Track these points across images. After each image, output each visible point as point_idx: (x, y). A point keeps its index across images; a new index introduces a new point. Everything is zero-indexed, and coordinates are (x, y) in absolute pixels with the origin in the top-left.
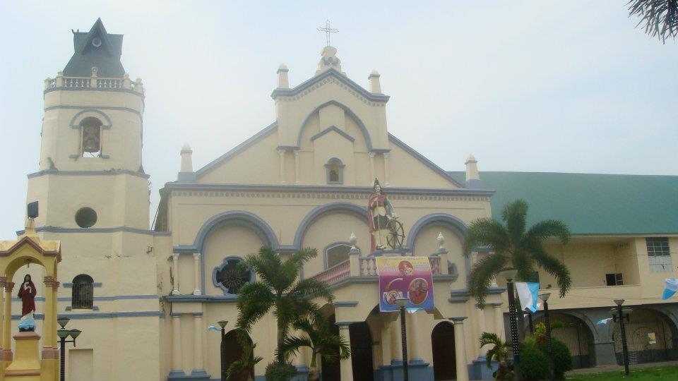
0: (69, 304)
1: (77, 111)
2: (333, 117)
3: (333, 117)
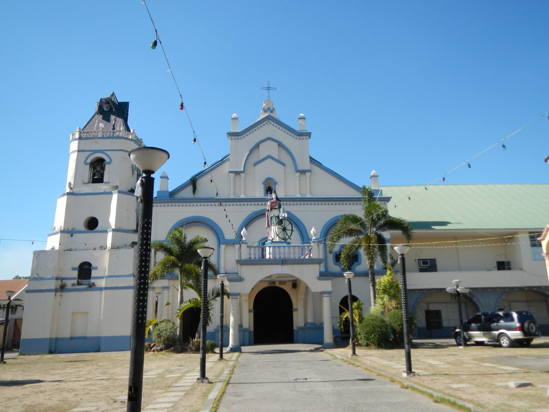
0: (75, 281)
1: (89, 153)
2: (269, 149)
3: (269, 149)
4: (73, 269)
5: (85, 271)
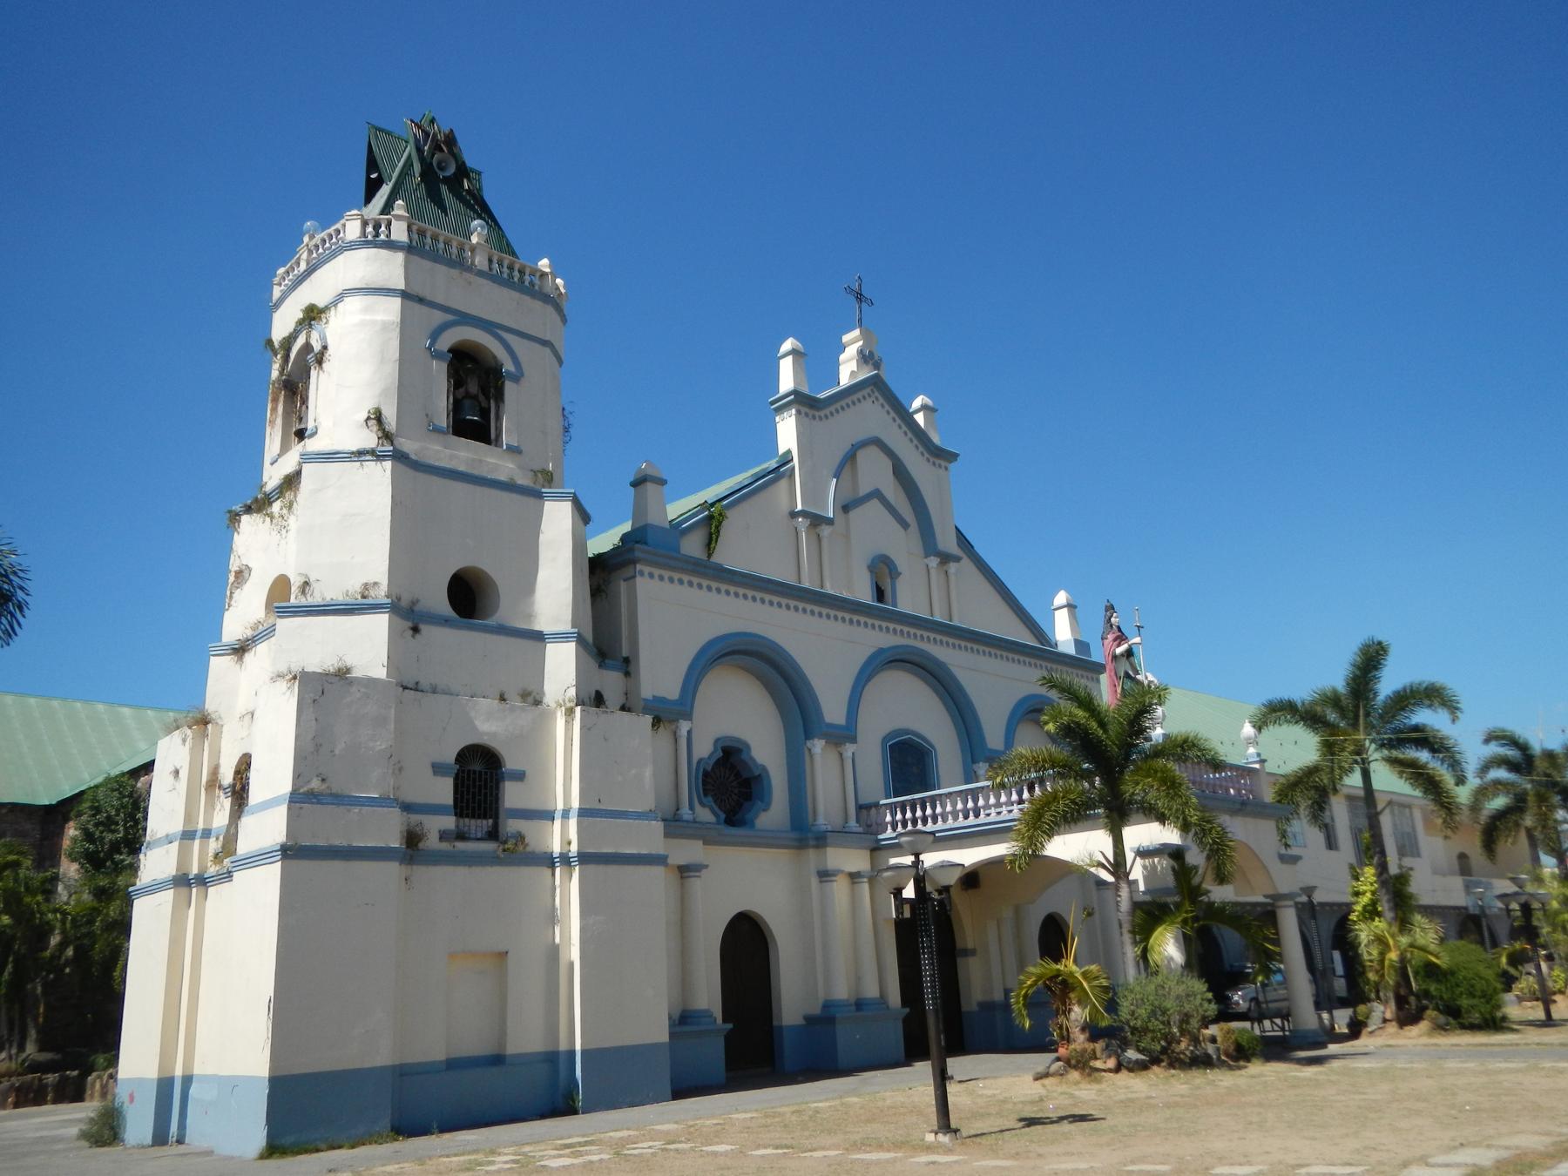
1: (439, 317)
2: (874, 472)
4: (438, 769)
5: (480, 781)
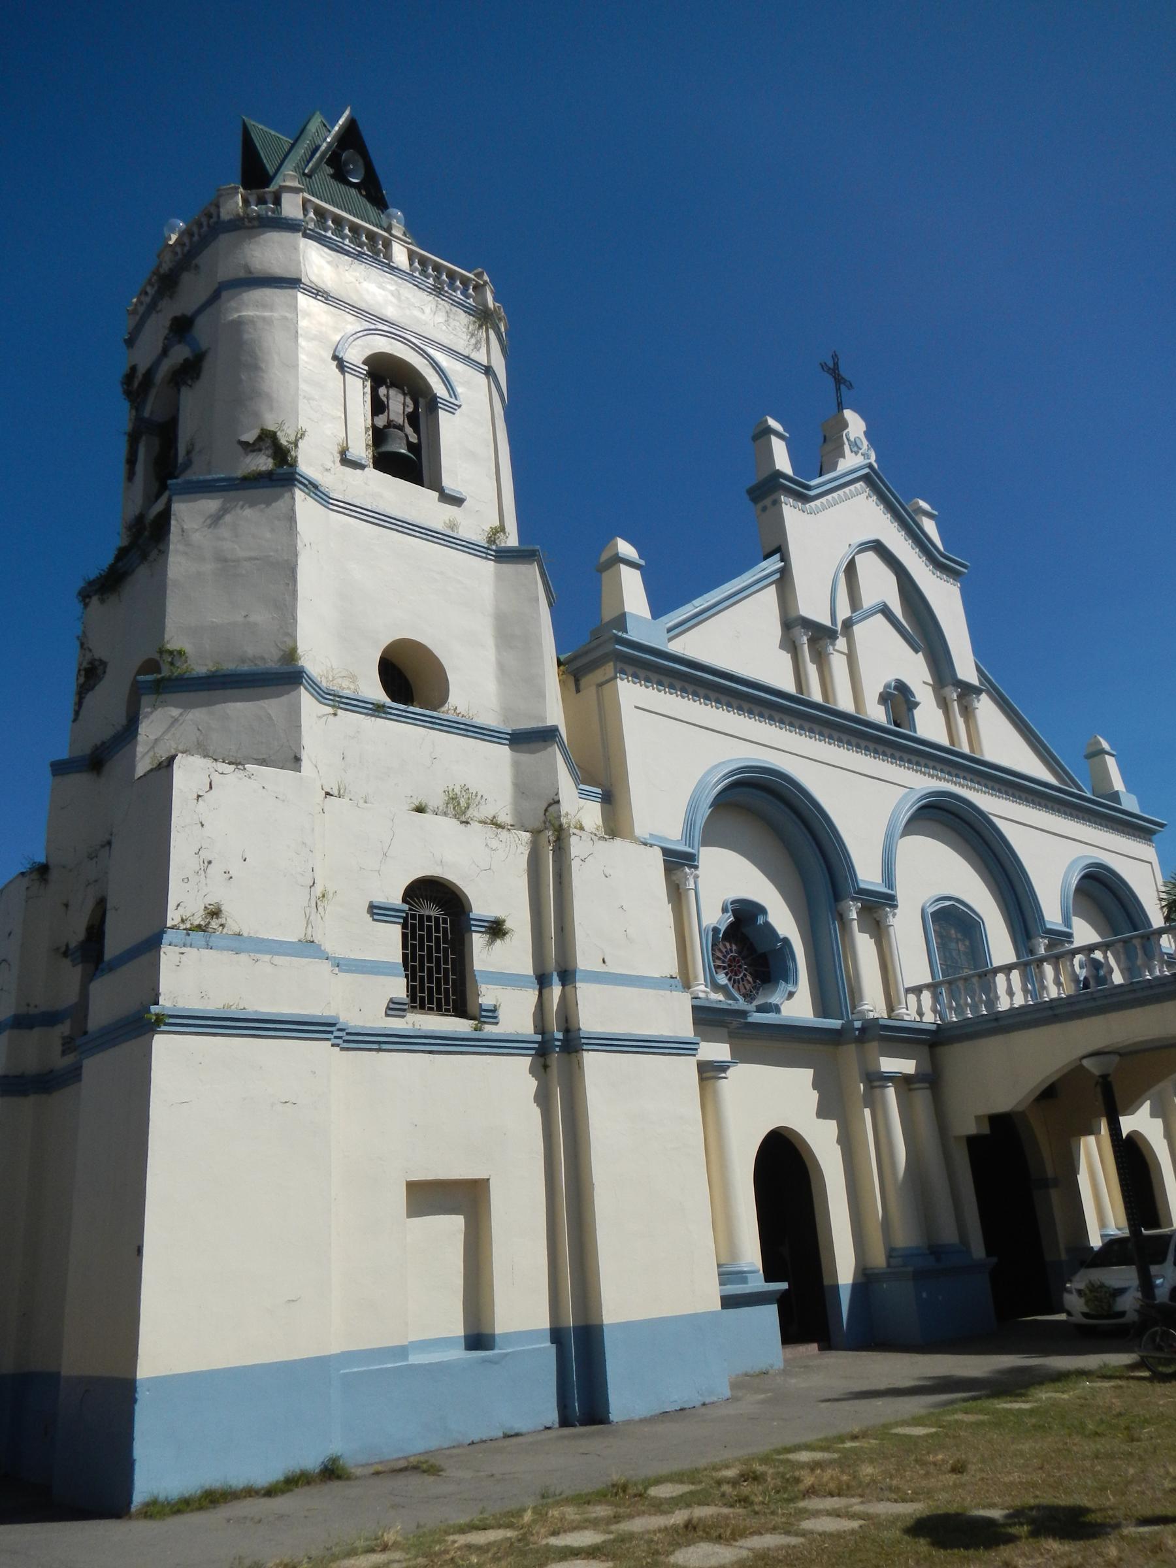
0: (398, 987)
